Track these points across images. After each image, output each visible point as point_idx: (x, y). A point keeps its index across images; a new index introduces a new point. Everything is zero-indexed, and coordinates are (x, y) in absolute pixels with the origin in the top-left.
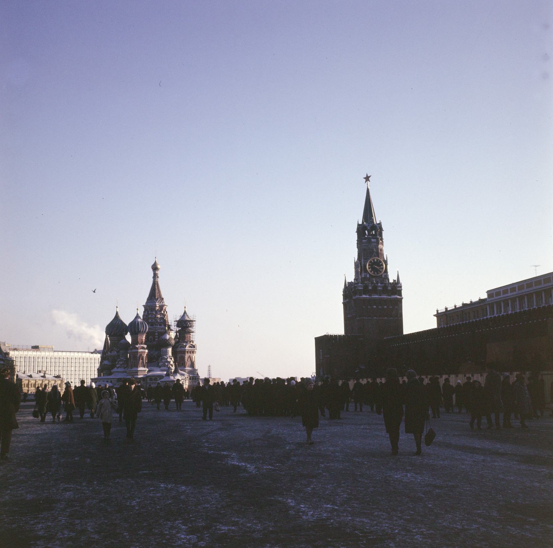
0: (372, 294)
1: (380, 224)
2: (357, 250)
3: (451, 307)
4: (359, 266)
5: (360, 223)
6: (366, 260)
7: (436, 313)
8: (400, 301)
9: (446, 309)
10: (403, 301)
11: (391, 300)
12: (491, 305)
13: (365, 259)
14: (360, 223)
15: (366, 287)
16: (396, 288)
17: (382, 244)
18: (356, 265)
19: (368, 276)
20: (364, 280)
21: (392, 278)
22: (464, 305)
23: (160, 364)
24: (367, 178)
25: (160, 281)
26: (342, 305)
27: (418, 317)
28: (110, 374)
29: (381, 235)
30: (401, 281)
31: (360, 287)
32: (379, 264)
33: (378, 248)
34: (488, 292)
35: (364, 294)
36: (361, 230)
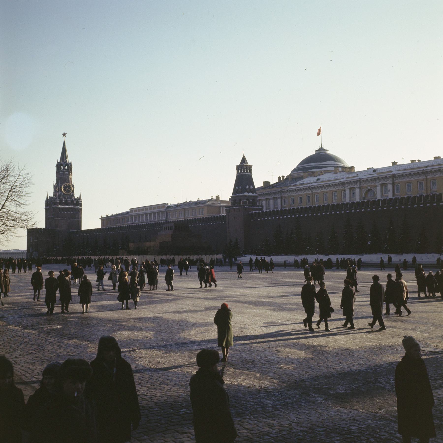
0: (64, 204)
1: (71, 163)
2: (56, 177)
3: (110, 215)
5: (59, 161)
6: (62, 184)
8: (81, 209)
11: (75, 209)
12: (132, 217)
13: (61, 184)
14: (59, 161)
16: (78, 202)
17: (72, 175)
18: (55, 187)
20: (60, 196)
21: (76, 196)
24: (64, 135)
26: (44, 210)
27: (90, 221)
29: (71, 170)
30: (82, 198)
32: (69, 187)
33: (69, 178)
34: (130, 209)
35: (60, 205)
36: (58, 165)
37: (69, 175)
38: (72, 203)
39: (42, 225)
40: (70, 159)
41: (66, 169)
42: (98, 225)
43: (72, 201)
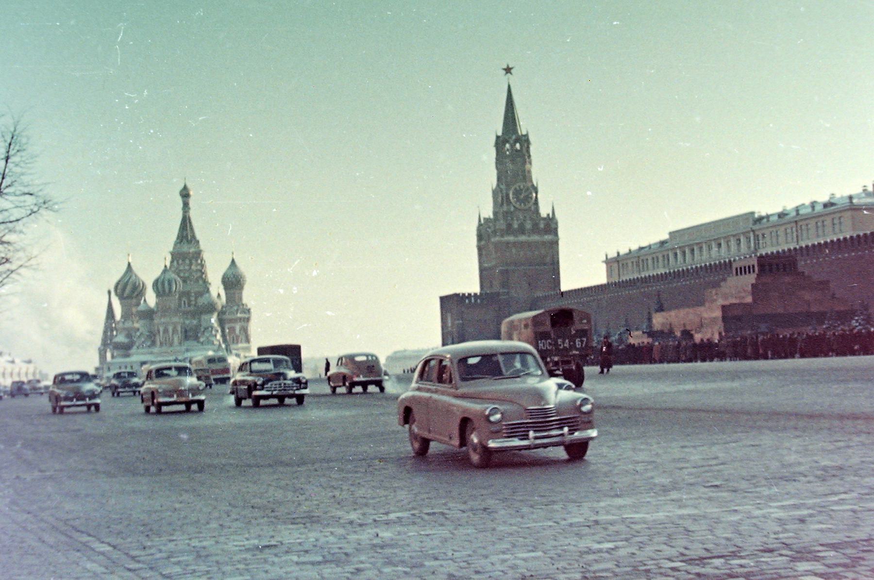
1: (527, 135)
3: (624, 251)
4: (500, 197)
5: (500, 134)
6: (508, 186)
7: (604, 259)
9: (618, 253)
10: (560, 243)
14: (500, 134)
15: (509, 226)
16: (550, 226)
17: (530, 163)
19: (512, 209)
22: (641, 248)
23: (202, 340)
24: (508, 70)
25: (193, 214)
28: (128, 356)
30: (558, 216)
31: (502, 224)
34: (670, 233)
36: (500, 143)
37: (524, 163)
38: (535, 229)
39: (471, 285)
40: (524, 126)
41: (517, 151)
42: (599, 277)
43: (535, 225)
